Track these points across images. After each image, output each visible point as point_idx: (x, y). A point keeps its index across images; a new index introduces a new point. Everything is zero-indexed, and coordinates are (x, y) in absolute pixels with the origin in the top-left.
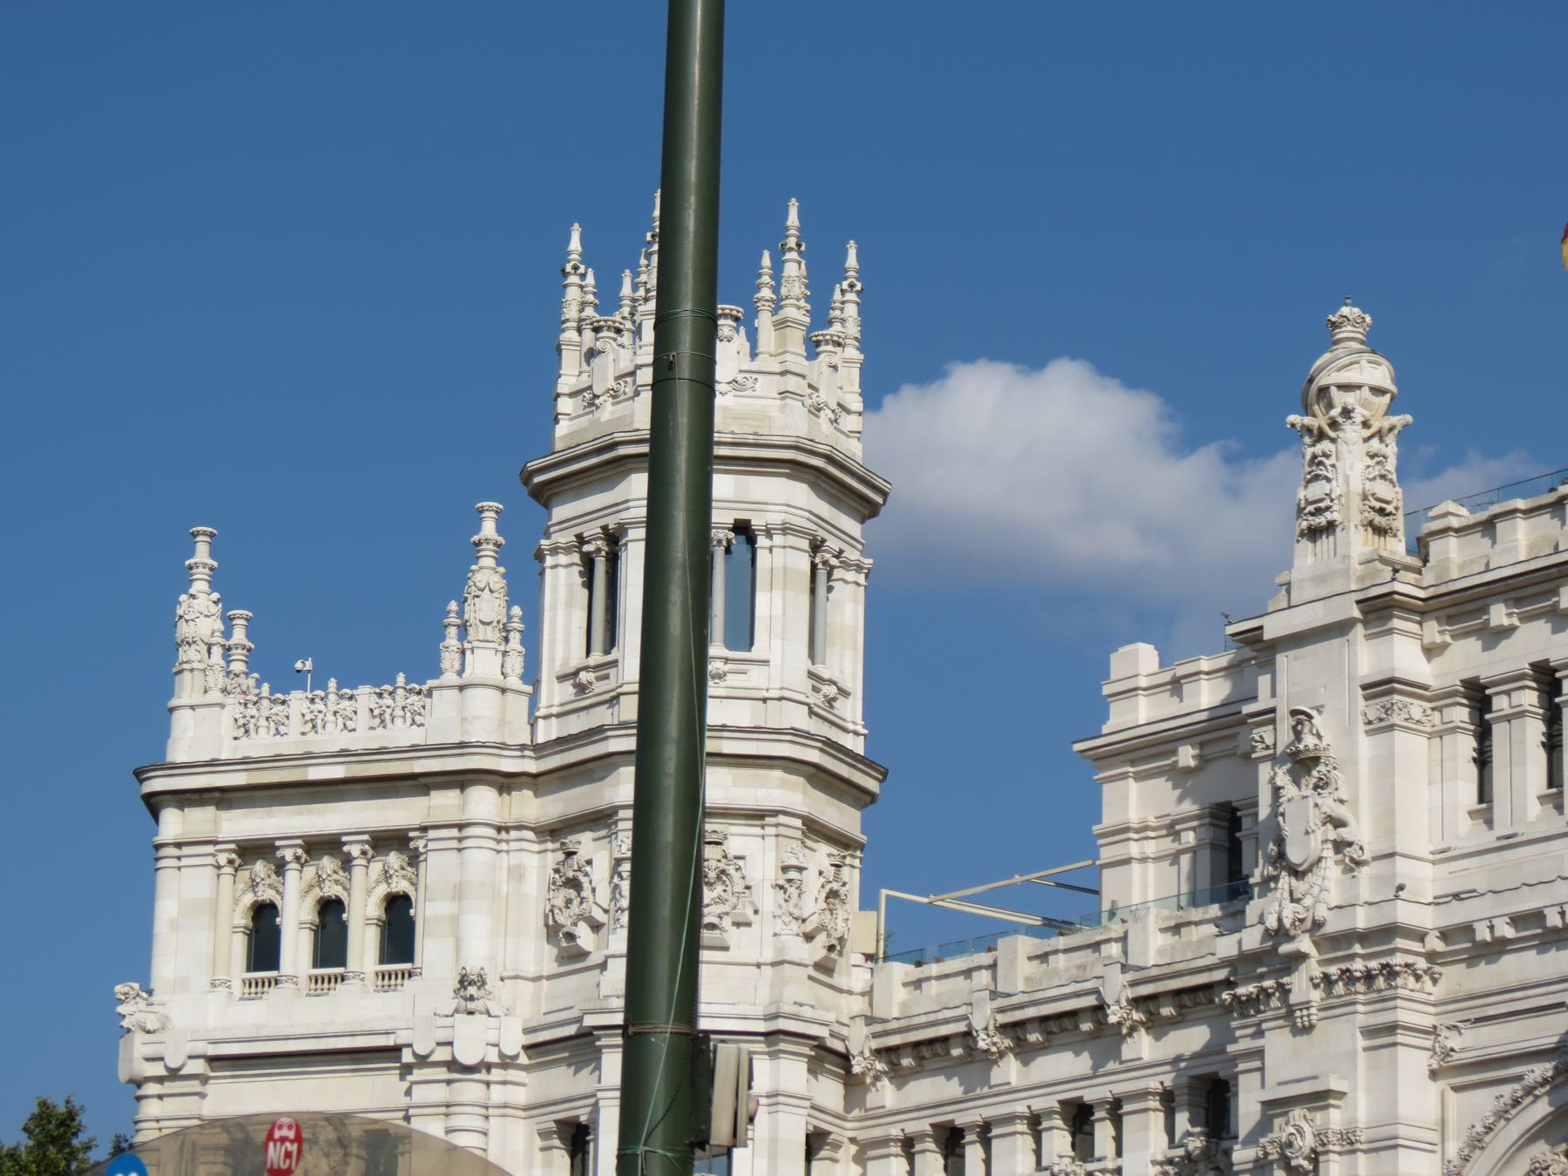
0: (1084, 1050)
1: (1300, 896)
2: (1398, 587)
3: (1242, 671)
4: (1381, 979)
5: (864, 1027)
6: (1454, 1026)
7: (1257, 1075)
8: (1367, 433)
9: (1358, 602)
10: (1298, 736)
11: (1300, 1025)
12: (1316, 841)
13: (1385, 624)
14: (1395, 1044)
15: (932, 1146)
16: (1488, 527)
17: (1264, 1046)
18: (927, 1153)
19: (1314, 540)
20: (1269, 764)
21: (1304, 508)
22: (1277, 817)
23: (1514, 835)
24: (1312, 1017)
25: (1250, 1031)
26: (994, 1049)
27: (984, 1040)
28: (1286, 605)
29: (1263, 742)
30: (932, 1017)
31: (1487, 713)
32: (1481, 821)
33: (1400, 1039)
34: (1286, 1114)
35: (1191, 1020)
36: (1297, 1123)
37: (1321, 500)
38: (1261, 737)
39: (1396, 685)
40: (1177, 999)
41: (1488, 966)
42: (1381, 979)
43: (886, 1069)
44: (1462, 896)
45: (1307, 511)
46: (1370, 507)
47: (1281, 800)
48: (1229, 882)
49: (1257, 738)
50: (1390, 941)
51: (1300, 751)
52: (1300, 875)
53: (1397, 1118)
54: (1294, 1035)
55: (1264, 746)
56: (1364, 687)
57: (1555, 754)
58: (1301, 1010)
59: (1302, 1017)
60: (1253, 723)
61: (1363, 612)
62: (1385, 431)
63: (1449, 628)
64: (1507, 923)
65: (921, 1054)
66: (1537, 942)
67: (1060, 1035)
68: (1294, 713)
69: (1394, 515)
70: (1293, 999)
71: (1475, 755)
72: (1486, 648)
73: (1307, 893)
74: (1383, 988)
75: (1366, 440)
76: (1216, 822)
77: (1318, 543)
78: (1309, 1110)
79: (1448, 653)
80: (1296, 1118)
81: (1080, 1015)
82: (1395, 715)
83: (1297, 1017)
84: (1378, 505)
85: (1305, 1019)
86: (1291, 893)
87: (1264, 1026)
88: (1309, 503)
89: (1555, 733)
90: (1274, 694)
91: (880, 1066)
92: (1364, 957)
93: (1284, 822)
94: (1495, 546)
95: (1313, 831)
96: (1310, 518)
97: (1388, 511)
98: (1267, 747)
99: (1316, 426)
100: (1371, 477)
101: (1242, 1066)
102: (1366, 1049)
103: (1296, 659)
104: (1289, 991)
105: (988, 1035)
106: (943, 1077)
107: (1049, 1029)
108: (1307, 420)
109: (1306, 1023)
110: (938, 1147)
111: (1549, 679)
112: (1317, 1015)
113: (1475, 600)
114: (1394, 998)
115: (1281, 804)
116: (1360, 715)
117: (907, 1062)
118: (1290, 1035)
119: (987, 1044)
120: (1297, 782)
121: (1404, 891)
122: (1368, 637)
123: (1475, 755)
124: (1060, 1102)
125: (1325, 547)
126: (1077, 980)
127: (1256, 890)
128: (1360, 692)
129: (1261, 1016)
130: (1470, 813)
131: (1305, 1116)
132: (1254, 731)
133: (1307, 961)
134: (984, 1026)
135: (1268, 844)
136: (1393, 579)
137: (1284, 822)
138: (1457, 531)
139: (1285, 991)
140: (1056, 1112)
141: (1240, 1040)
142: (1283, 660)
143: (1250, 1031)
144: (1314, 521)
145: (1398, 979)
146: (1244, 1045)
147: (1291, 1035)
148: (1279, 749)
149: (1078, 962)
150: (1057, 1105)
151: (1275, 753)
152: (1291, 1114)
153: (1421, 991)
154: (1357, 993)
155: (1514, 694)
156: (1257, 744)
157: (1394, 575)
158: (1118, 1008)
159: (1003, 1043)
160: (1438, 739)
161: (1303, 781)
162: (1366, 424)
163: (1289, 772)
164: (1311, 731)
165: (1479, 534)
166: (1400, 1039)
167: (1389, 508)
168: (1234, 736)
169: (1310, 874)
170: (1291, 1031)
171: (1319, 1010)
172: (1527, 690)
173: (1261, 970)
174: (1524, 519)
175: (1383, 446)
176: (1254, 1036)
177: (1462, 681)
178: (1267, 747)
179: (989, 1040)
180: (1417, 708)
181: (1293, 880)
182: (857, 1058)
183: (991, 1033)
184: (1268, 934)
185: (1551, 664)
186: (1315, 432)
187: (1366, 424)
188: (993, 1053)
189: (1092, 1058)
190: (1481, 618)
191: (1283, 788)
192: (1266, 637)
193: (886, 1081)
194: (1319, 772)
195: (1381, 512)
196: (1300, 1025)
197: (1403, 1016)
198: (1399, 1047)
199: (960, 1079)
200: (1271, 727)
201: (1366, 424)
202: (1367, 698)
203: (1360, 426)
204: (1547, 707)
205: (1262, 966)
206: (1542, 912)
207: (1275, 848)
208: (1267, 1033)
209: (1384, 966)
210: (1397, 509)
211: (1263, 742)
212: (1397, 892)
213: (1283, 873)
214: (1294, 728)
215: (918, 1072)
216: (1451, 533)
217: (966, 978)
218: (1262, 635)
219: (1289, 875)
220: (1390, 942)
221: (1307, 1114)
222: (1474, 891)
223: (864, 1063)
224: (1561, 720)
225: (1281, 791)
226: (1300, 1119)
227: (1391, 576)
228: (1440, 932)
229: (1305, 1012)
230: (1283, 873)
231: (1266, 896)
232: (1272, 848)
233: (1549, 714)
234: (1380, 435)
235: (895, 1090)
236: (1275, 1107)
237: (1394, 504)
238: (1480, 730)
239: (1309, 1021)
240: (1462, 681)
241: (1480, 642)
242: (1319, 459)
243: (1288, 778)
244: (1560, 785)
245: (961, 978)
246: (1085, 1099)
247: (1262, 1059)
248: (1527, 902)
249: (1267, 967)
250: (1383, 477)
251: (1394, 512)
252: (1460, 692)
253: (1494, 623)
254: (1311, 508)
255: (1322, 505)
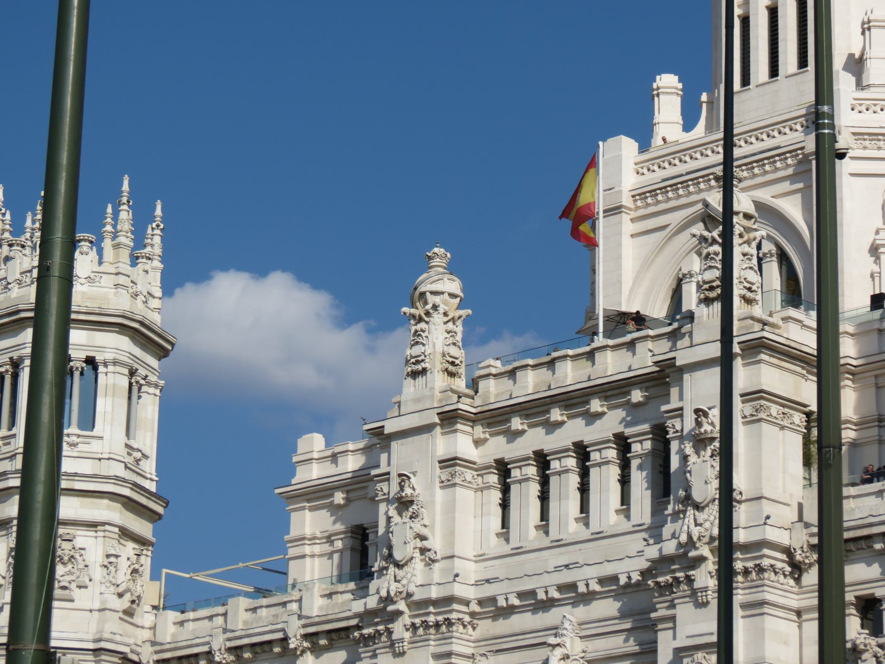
0: (875, 562)
1: (400, 579)
2: (765, 334)
3: (372, 451)
4: (754, 574)
5: (297, 621)
6: (484, 654)
7: (671, 632)
8: (446, 319)
9: (739, 343)
10: (699, 424)
11: (701, 601)
12: (712, 487)
13: (755, 358)
14: (763, 614)
15: (854, 612)
16: (631, 345)
17: (675, 614)
18: (852, 616)
19: (708, 306)
20: (677, 441)
21: (702, 286)
22: (388, 534)
23: (602, 532)
24: (709, 597)
25: (370, 654)
26: (807, 561)
27: (800, 555)
28: (398, 415)
29: (382, 491)
30: (860, 522)
31: (587, 462)
32: (582, 523)
33: (766, 610)
34: (693, 655)
35: (852, 560)
36: (700, 661)
37: (713, 281)
38: (673, 425)
39: (762, 394)
40: (329, 635)
41: (584, 607)
42: (754, 574)
43: (310, 646)
44: (491, 581)
45: (703, 288)
46: (446, 361)
47: (688, 463)
48: (361, 568)
49: (670, 426)
50: (760, 550)
51: (701, 434)
52: (400, 567)
53: (765, 659)
54: (696, 608)
55: (675, 430)
56: (742, 396)
57: (545, 502)
58: (701, 592)
59: (399, 647)
60: (666, 417)
61: (742, 350)
62: (456, 318)
63: (488, 430)
64: (516, 597)
65: (332, 637)
66: (613, 594)
67: (857, 552)
68: (697, 411)
69: (756, 292)
70: (696, 585)
71: (579, 486)
72: (587, 425)
73: (404, 577)
74: (755, 579)
75: (740, 245)
76: (354, 535)
77: (711, 307)
78: (707, 653)
79: (605, 418)
80: (699, 657)
81: (874, 538)
82: (762, 413)
83: (699, 596)
84: (748, 285)
85: (704, 597)
86: (695, 520)
87: (378, 652)
88: (705, 282)
89: (626, 475)
90: (681, 398)
91: (306, 644)
92: (742, 560)
93: (691, 476)
94: (594, 367)
95: (711, 482)
96: (706, 292)
97: (752, 290)
98: (384, 494)
99: (418, 314)
100: (744, 268)
101: (660, 627)
102: (743, 617)
103: (402, 445)
104: (694, 580)
105: (803, 551)
106: (864, 564)
107: (849, 548)
108: (706, 233)
109: (705, 600)
110: (857, 612)
111: (543, 460)
112: (711, 595)
113: (584, 396)
114: (451, 638)
115: (391, 527)
116: (739, 413)
117: (323, 642)
118: (392, 657)
119: (802, 557)
120: (697, 453)
121: (770, 519)
122: (443, 434)
123: (579, 486)
124: (856, 597)
125: (711, 312)
126: (509, 577)
127: (669, 518)
128: (739, 399)
129: (376, 646)
130: (575, 519)
131: (704, 657)
132: (669, 422)
133: (706, 562)
134: (801, 545)
135: (679, 490)
136: (763, 330)
137: (691, 476)
138: (652, 337)
139: (690, 580)
140: (852, 604)
141: (364, 660)
142: (686, 377)
143: (666, 604)
144: (709, 294)
145: (765, 573)
146: (662, 613)
147: (694, 607)
148: (685, 433)
149: (273, 613)
150: (854, 599)
151: (389, 498)
152: (695, 656)
153: (778, 582)
154: (430, 634)
155: (603, 451)
156: (670, 429)
157: (763, 326)
158: (295, 639)
159: (813, 557)
160: (480, 492)
161: (702, 453)
162: (445, 314)
163: (694, 447)
164: (708, 423)
165: (666, 339)
166: (766, 610)
167: (754, 288)
168: (366, 487)
169: (707, 508)
170: (392, 655)
171: (713, 592)
172: (611, 449)
173: (673, 567)
174: (532, 370)
175: (750, 249)
176: (668, 608)
177: (573, 443)
178: (677, 431)
179: (804, 555)
180: (775, 409)
181: (697, 513)
182: (292, 639)
183: (805, 550)
184: (680, 545)
185: (545, 452)
186: (710, 240)
187: (741, 236)
188: (806, 564)
189: (880, 567)
190: (585, 407)
191: (690, 455)
192: (678, 363)
193: (309, 653)
194: (714, 446)
195: (749, 289)
196: (701, 601)
197: (456, 648)
198: (765, 615)
199: (879, 564)
200: (679, 419)
201: (445, 314)
202: (441, 468)
203: (738, 236)
204: (541, 475)
205: (674, 565)
206: (617, 576)
207: (684, 493)
208: (677, 606)
209: (446, 619)
210: (758, 288)
211: (382, 491)
212: (766, 520)
213: (391, 565)
214: (696, 420)
215: (329, 649)
216: (491, 377)
217: (877, 497)
218: (675, 363)
219: (395, 567)
220: (760, 551)
221: (706, 655)
222: (577, 563)
223: (298, 643)
224: (549, 483)
225: (689, 457)
226: (701, 659)
227: (761, 327)
228: (598, 580)
229: (704, 594)
230: (391, 565)
231: (380, 578)
232: (682, 493)
233: (543, 480)
234: (748, 242)
235: (315, 659)
236: (680, 653)
237: (757, 285)
238: (504, 488)
239: (707, 599)
240: (573, 443)
241: (584, 421)
242: (712, 256)
243: (692, 449)
244: (629, 504)
245: (873, 497)
246: (876, 595)
247: (674, 622)
248: (527, 585)
249: (679, 565)
250: (751, 268)
251: (460, 364)
252: (571, 449)
253: (513, 428)
254: (706, 286)
255: (420, 359)
